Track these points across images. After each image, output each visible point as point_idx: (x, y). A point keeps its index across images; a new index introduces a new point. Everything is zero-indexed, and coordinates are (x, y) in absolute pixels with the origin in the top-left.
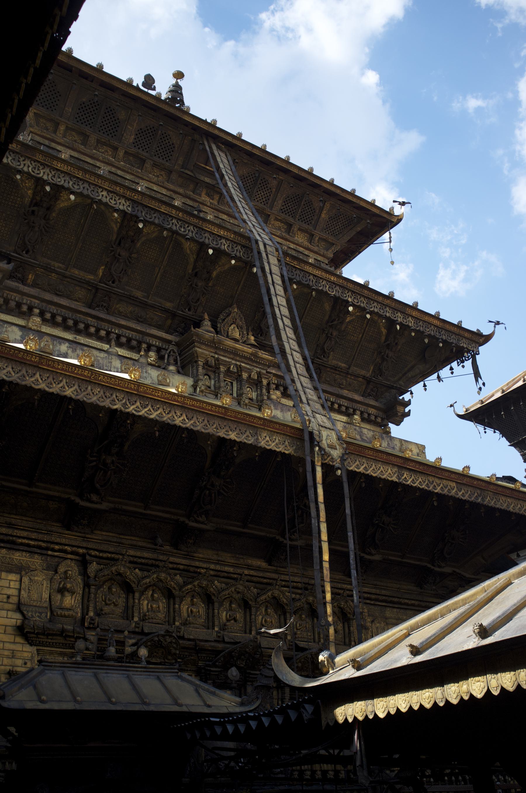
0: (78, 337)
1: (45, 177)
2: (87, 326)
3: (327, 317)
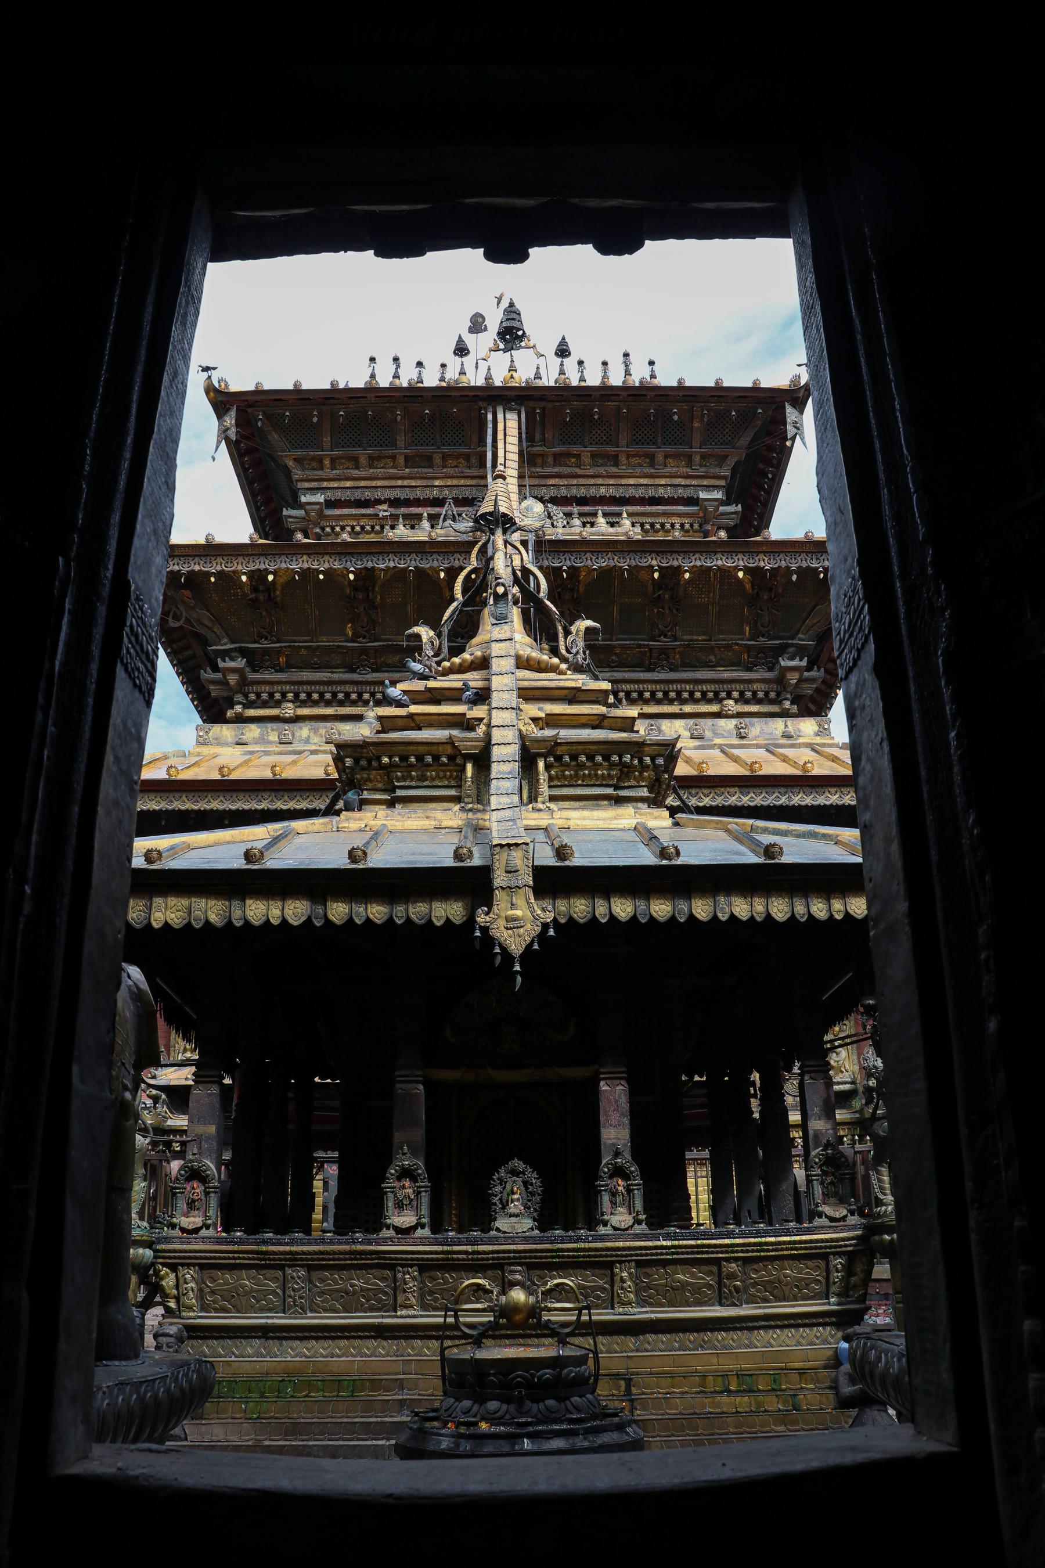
0: (339, 709)
1: (240, 568)
2: (347, 695)
3: (651, 588)
